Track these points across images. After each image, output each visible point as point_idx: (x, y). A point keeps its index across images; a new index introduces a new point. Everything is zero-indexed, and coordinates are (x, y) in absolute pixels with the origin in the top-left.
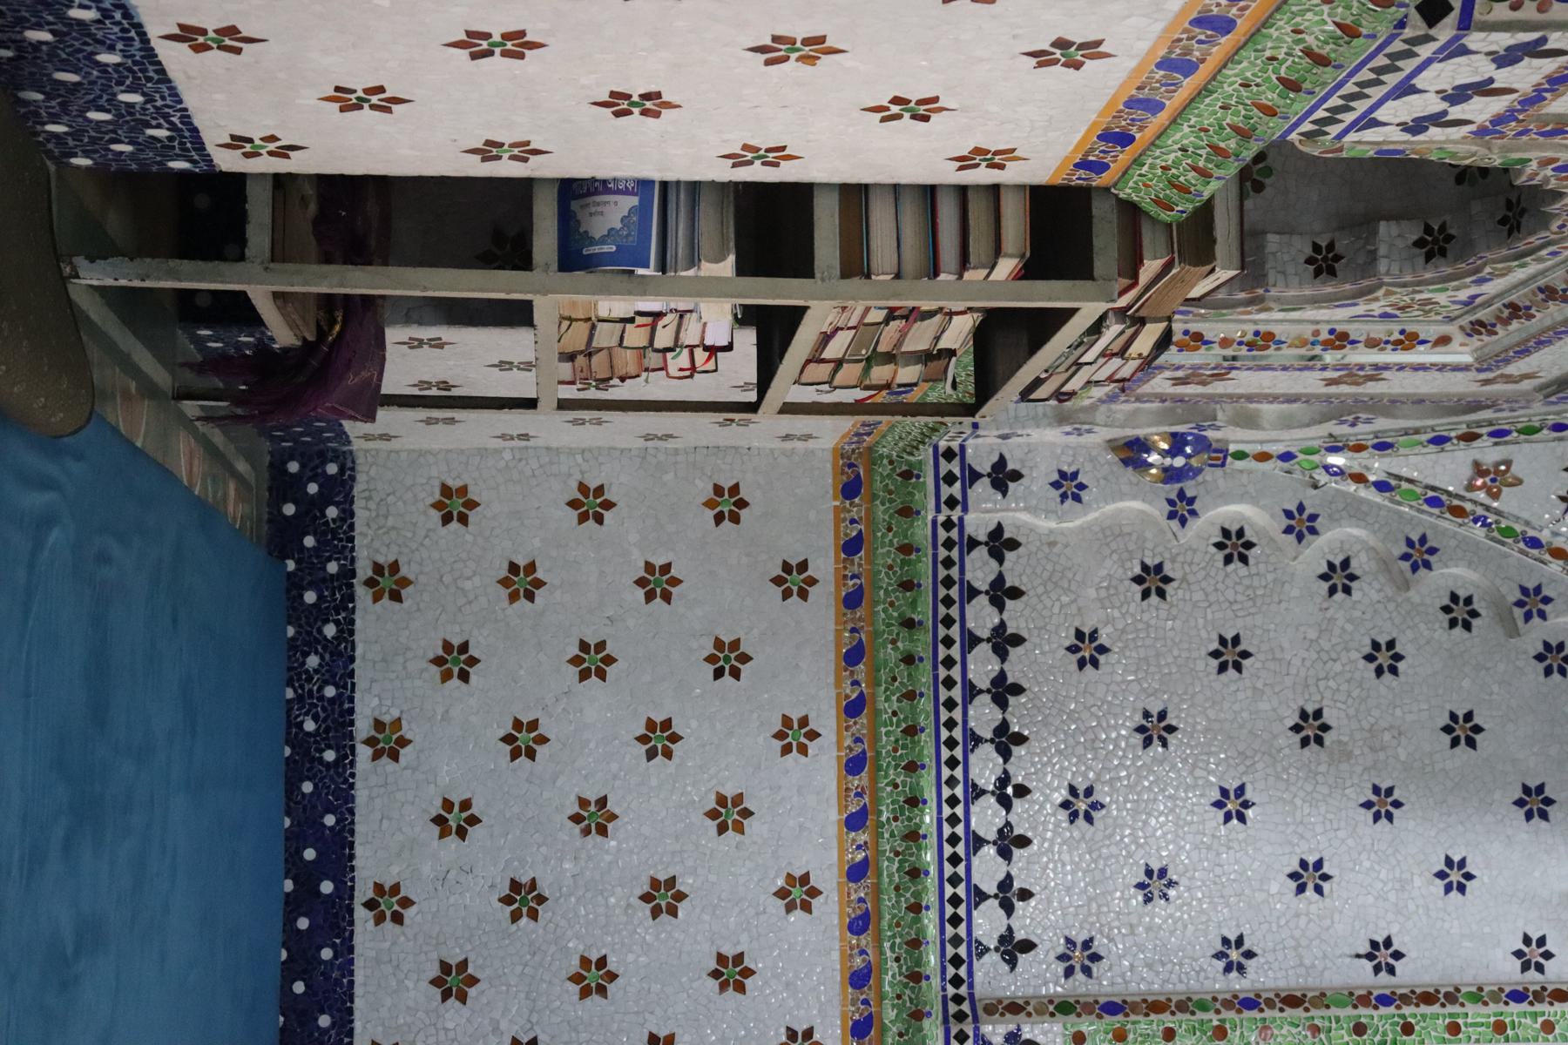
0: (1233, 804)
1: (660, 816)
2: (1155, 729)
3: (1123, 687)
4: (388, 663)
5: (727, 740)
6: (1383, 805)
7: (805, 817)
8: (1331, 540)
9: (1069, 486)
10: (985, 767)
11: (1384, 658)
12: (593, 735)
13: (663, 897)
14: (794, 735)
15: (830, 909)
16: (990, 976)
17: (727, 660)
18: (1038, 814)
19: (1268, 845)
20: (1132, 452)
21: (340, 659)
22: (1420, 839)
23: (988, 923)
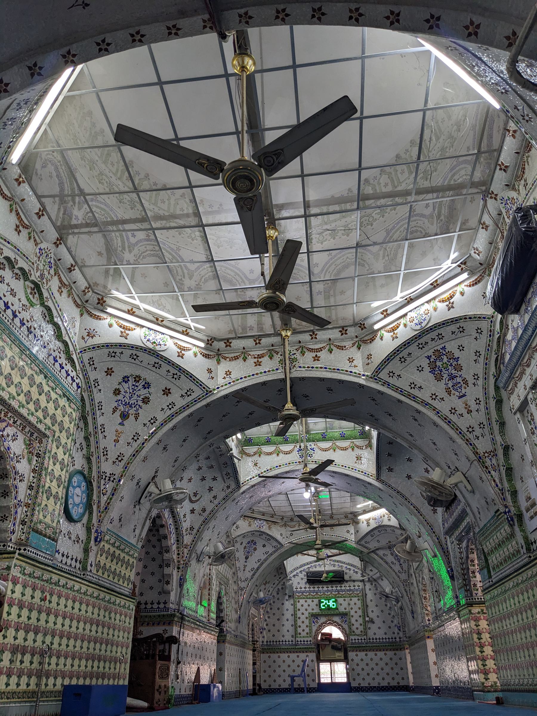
0: (283, 625)
1: (284, 666)
2: (279, 631)
3: (276, 634)
4: (275, 686)
5: (279, 661)
6: (283, 615)
7: (284, 656)
8: (267, 618)
9: (263, 637)
10: (281, 643)
11: (274, 614)
12: (279, 671)
13: (289, 666)
14: (279, 657)
15: (290, 654)
16: (294, 643)
17: (274, 662)
18: (284, 639)
19: (286, 623)
20: (261, 633)
21: (275, 689)
22: (285, 612)
23: (291, 643)
